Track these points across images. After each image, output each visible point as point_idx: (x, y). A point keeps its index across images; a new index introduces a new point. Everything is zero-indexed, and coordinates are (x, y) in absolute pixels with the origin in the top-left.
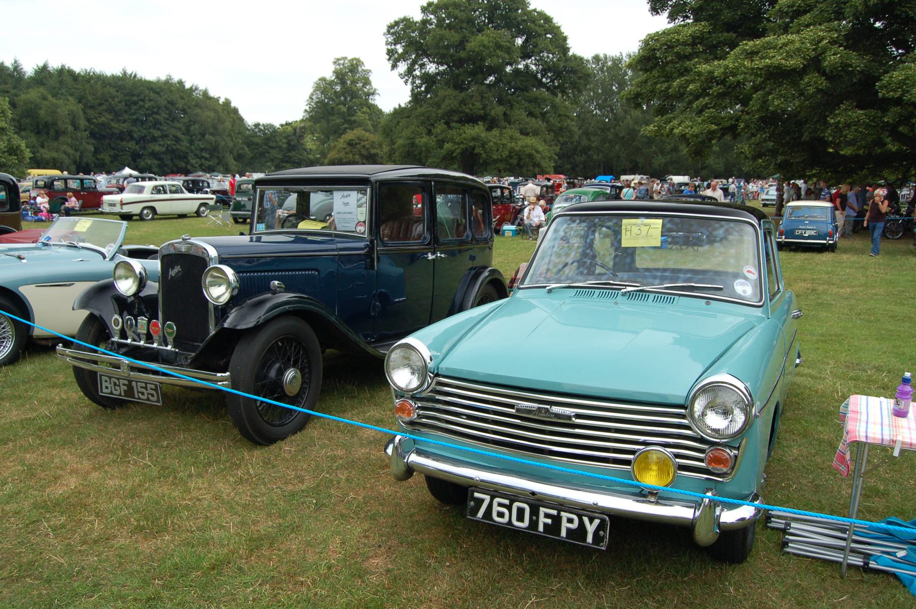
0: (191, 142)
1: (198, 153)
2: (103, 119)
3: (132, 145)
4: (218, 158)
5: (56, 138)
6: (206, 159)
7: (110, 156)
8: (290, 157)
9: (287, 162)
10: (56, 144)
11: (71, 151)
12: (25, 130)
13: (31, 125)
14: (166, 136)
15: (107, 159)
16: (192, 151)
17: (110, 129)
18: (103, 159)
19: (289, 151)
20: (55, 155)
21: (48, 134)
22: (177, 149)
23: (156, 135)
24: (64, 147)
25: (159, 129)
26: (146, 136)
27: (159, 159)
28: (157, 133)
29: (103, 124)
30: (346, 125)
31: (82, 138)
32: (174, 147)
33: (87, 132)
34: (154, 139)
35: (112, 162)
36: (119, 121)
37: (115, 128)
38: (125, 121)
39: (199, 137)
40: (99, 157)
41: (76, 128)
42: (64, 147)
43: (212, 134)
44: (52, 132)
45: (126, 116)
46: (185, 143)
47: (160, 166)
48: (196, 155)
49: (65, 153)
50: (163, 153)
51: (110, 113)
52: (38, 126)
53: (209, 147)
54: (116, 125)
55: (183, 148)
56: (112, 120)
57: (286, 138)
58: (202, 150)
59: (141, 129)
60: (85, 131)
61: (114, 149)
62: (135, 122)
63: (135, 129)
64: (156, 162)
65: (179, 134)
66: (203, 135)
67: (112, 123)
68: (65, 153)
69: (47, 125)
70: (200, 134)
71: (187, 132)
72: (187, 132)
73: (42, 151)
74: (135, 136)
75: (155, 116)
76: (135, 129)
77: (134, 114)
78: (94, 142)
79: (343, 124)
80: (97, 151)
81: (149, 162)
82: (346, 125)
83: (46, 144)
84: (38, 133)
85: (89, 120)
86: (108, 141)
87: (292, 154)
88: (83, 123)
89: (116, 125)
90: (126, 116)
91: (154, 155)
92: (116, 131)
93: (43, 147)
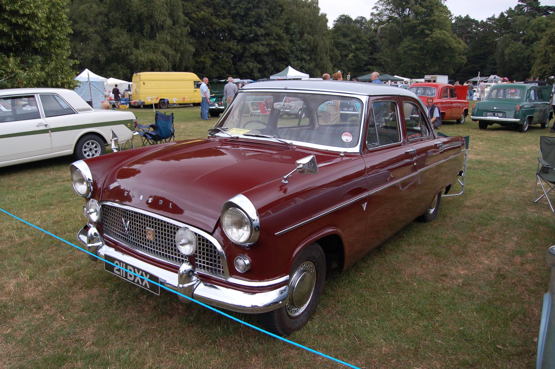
0: (291, 41)
1: (298, 53)
2: (202, 13)
3: (233, 44)
4: (315, 60)
5: (152, 37)
6: (306, 61)
7: (211, 58)
8: (375, 59)
9: (370, 64)
10: (152, 43)
11: (170, 52)
12: (114, 26)
13: (122, 21)
14: (267, 35)
15: (208, 62)
16: (292, 51)
17: (211, 26)
18: (204, 63)
19: (372, 54)
20: (152, 56)
21: (141, 31)
22: (280, 50)
23: (259, 33)
24: (163, 47)
25: (262, 27)
26: (247, 35)
27: (261, 62)
28: (261, 31)
29: (203, 19)
30: (422, 26)
31: (182, 34)
32: (278, 48)
33: (188, 28)
34: (256, 38)
35: (212, 66)
36: (218, 16)
37: (215, 24)
38: (224, 17)
39: (298, 36)
40: (199, 60)
41: (174, 23)
42: (163, 47)
43: (309, 33)
44: (147, 27)
45: (226, 12)
46: (287, 43)
47: (260, 71)
48: (296, 56)
49: (164, 53)
50: (267, 55)
51: (209, 7)
52: (129, 21)
53: (309, 48)
54: (217, 21)
55: (287, 49)
56: (212, 15)
57: (369, 39)
58: (302, 50)
59: (241, 25)
60: (185, 26)
61: (214, 50)
62: (234, 17)
63: (235, 26)
64: (259, 66)
65: (281, 32)
66: (302, 34)
67: (213, 19)
68: (164, 53)
69: (140, 19)
70: (299, 32)
71: (287, 30)
72: (287, 30)
73: (135, 51)
74: (237, 34)
75: (256, 10)
76: (235, 26)
77: (232, 9)
78: (194, 41)
79: (419, 26)
80: (196, 55)
81: (251, 65)
82: (422, 26)
83: (141, 44)
84: (130, 31)
85: (186, 14)
86: (208, 40)
87: (377, 55)
88: (182, 17)
89: (217, 21)
90: (226, 12)
91: (256, 56)
92: (217, 28)
93: (137, 46)
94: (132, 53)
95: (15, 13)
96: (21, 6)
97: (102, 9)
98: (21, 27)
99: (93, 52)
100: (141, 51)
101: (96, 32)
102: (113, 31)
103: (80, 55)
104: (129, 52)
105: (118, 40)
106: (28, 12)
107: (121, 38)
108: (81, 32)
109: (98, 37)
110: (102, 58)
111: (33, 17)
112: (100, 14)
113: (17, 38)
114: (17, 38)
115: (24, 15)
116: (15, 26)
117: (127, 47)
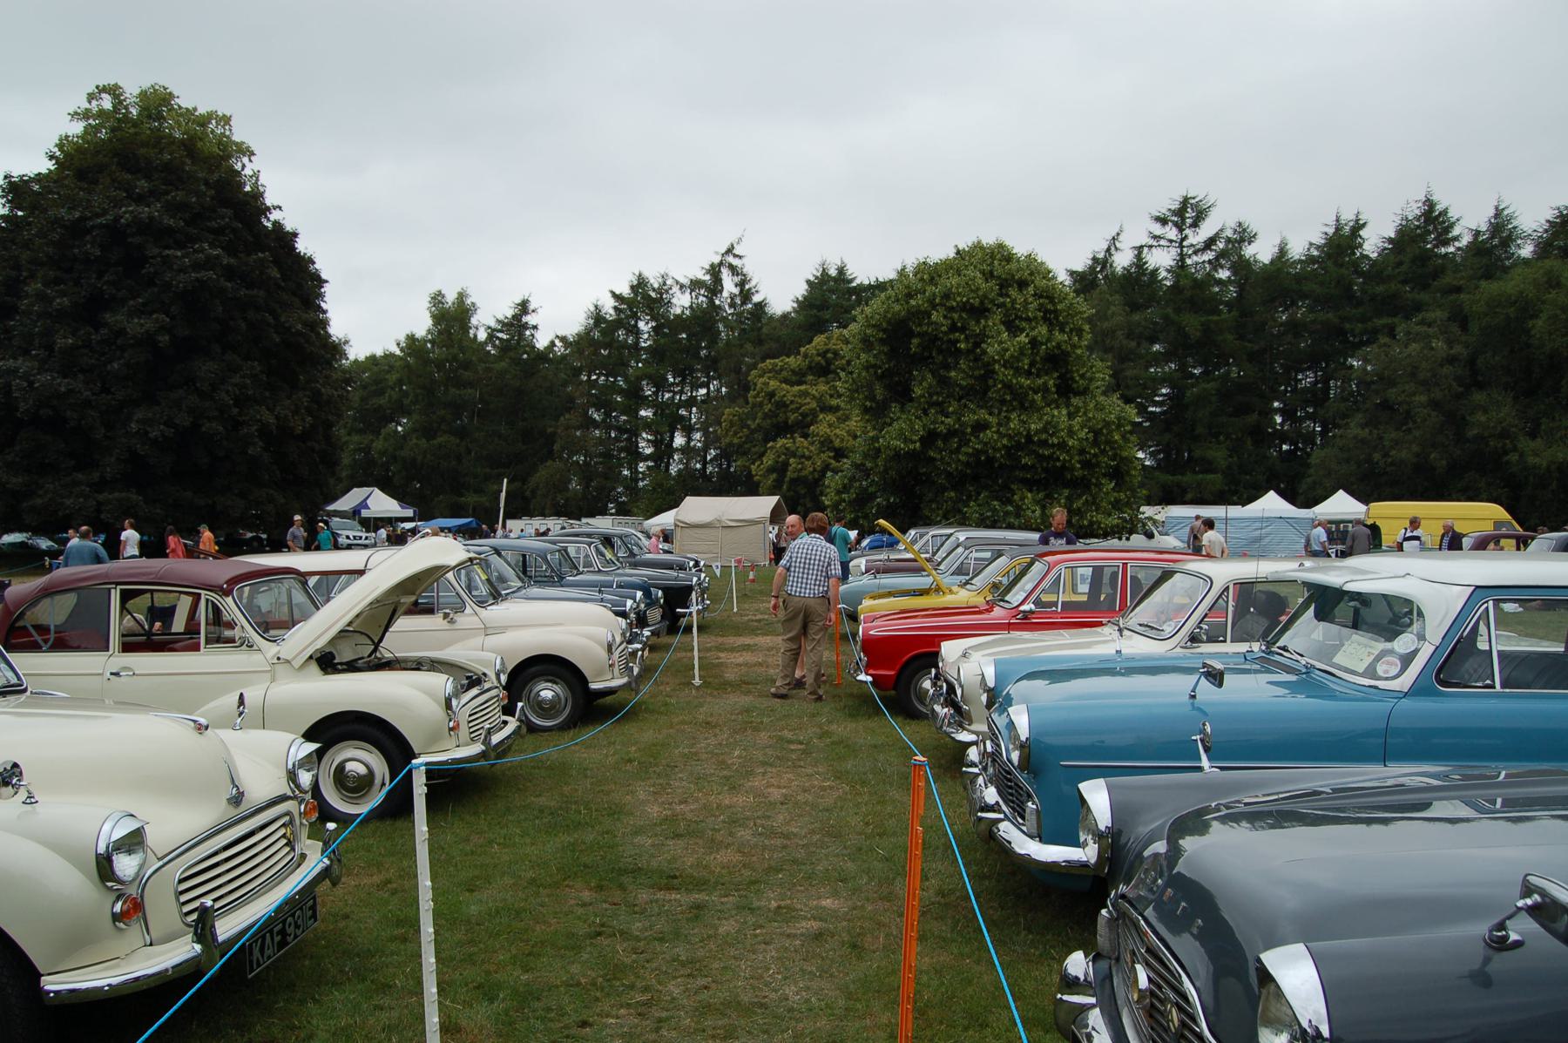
12: (1481, 386)
73: (1525, 444)
93: (1533, 435)
94: (1515, 449)
95: (1044, 443)
96: (1051, 436)
97: (1458, 349)
98: (1050, 457)
99: (1415, 448)
100: (1538, 443)
101: (1435, 404)
102: (1479, 397)
103: (1386, 455)
104: (1509, 446)
105: (1483, 419)
106: (1056, 441)
107: (1493, 412)
108: (1400, 404)
109: (1434, 414)
110: (1438, 460)
111: (1062, 445)
112: (1451, 360)
113: (1046, 470)
114: (1046, 470)
115: (1053, 445)
116: (1041, 458)
117: (1505, 434)
